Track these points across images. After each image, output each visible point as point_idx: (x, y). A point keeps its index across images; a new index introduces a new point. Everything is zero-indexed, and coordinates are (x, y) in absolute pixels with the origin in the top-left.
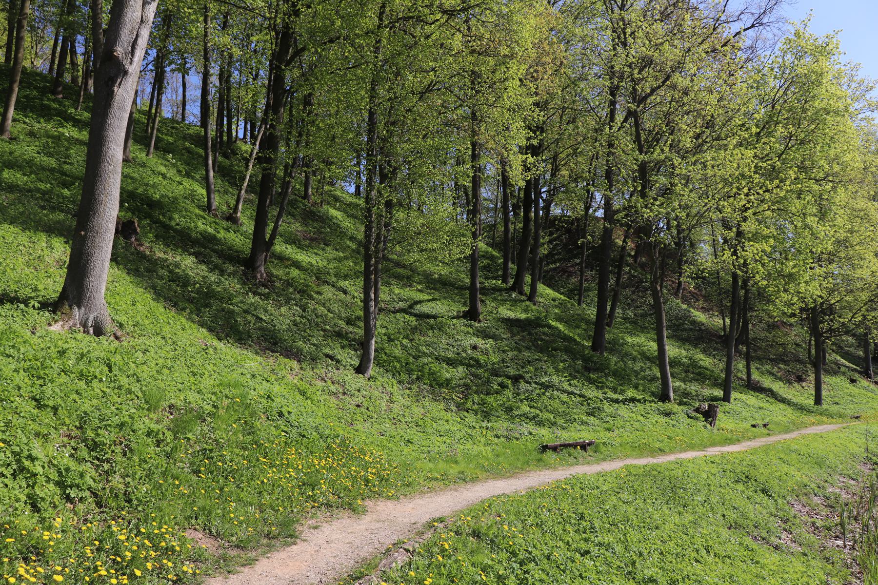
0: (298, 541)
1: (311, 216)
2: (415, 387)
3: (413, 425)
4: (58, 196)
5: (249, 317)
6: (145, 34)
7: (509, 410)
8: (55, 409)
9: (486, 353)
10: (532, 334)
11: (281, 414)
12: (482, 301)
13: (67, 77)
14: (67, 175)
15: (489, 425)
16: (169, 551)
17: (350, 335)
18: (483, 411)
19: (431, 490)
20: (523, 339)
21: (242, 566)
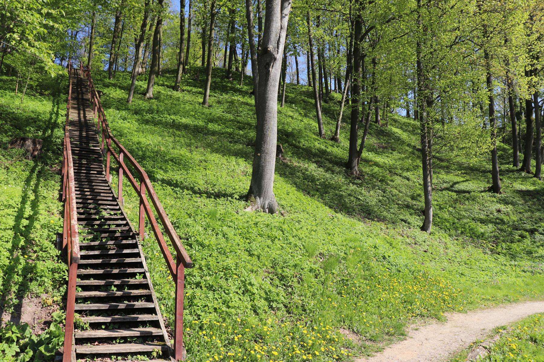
0: (407, 338)
1: (381, 133)
2: (460, 238)
3: (463, 263)
4: (237, 135)
5: (352, 198)
6: (284, 34)
7: (530, 253)
8: (259, 257)
9: (508, 214)
10: (540, 200)
11: (384, 258)
12: (501, 180)
13: (234, 69)
14: (240, 123)
15: (516, 263)
16: (331, 341)
17: (415, 207)
18: (510, 254)
19: (487, 307)
20: (534, 204)
21: (375, 352)
